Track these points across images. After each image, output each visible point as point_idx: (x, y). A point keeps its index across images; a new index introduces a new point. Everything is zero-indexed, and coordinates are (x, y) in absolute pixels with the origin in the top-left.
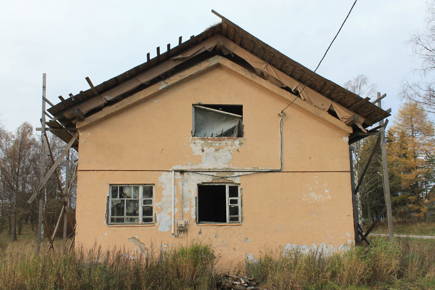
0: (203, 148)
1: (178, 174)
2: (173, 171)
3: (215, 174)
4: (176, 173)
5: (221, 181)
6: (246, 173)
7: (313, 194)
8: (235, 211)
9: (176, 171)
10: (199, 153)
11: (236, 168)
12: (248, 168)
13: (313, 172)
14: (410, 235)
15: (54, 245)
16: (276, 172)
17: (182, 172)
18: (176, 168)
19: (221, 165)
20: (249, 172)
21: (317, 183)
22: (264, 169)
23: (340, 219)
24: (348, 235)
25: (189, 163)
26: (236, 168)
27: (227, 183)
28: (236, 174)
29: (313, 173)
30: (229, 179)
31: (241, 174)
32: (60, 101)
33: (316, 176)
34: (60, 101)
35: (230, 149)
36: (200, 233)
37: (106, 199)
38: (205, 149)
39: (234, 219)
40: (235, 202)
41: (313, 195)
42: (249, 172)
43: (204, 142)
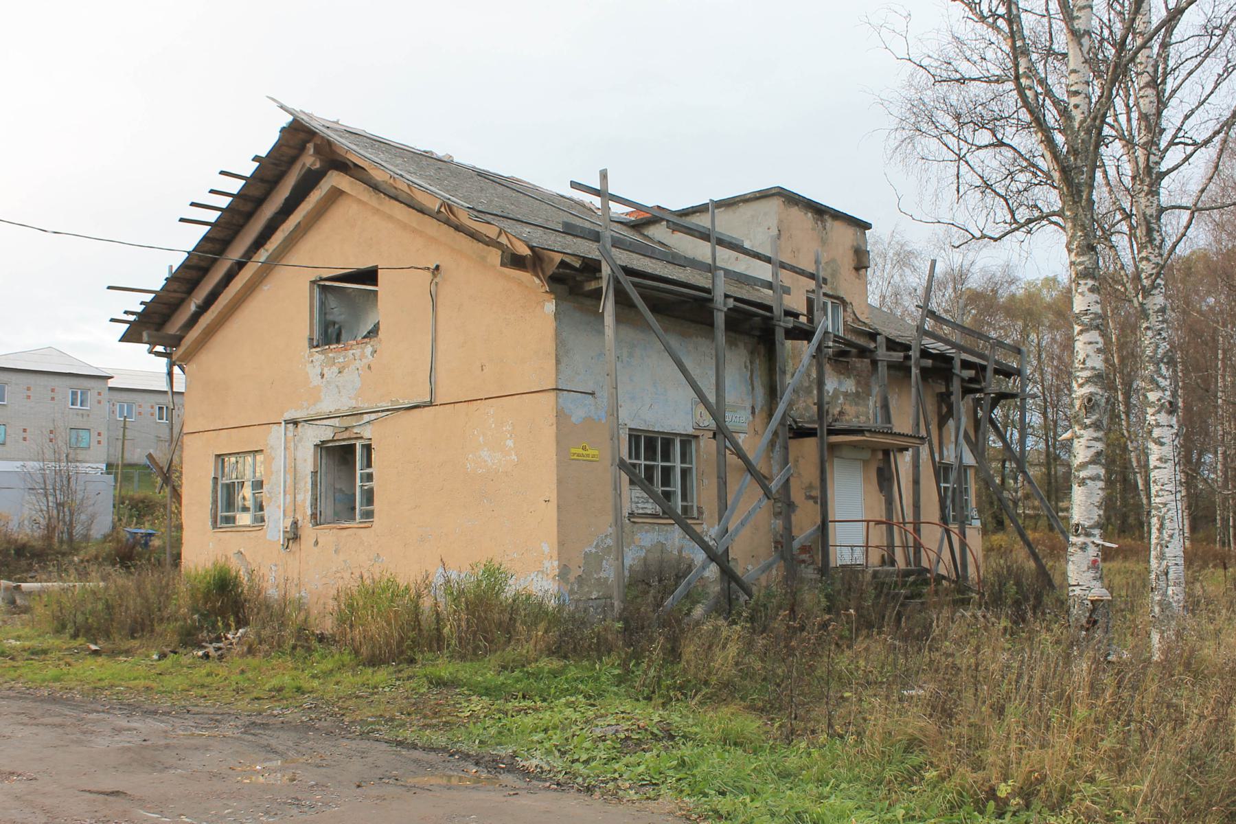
0: (322, 370)
1: (291, 426)
2: (283, 423)
3: (336, 422)
4: (288, 425)
5: (345, 435)
6: (380, 414)
7: (485, 453)
8: (369, 497)
9: (287, 422)
10: (316, 381)
11: (366, 405)
12: (384, 404)
13: (486, 399)
14: (1076, 462)
15: (306, 483)
16: (425, 406)
17: (295, 423)
18: (288, 416)
19: (345, 403)
20: (383, 411)
21: (493, 426)
22: (406, 401)
23: (531, 510)
24: (546, 548)
25: (305, 404)
26: (365, 405)
27: (356, 438)
28: (366, 418)
29: (487, 401)
30: (355, 430)
31: (373, 416)
32: (257, 164)
33: (491, 408)
34: (257, 164)
35: (358, 366)
36: (316, 543)
37: (211, 482)
38: (326, 370)
39: (369, 515)
40: (370, 477)
41: (485, 454)
42: (383, 411)
43: (323, 357)
